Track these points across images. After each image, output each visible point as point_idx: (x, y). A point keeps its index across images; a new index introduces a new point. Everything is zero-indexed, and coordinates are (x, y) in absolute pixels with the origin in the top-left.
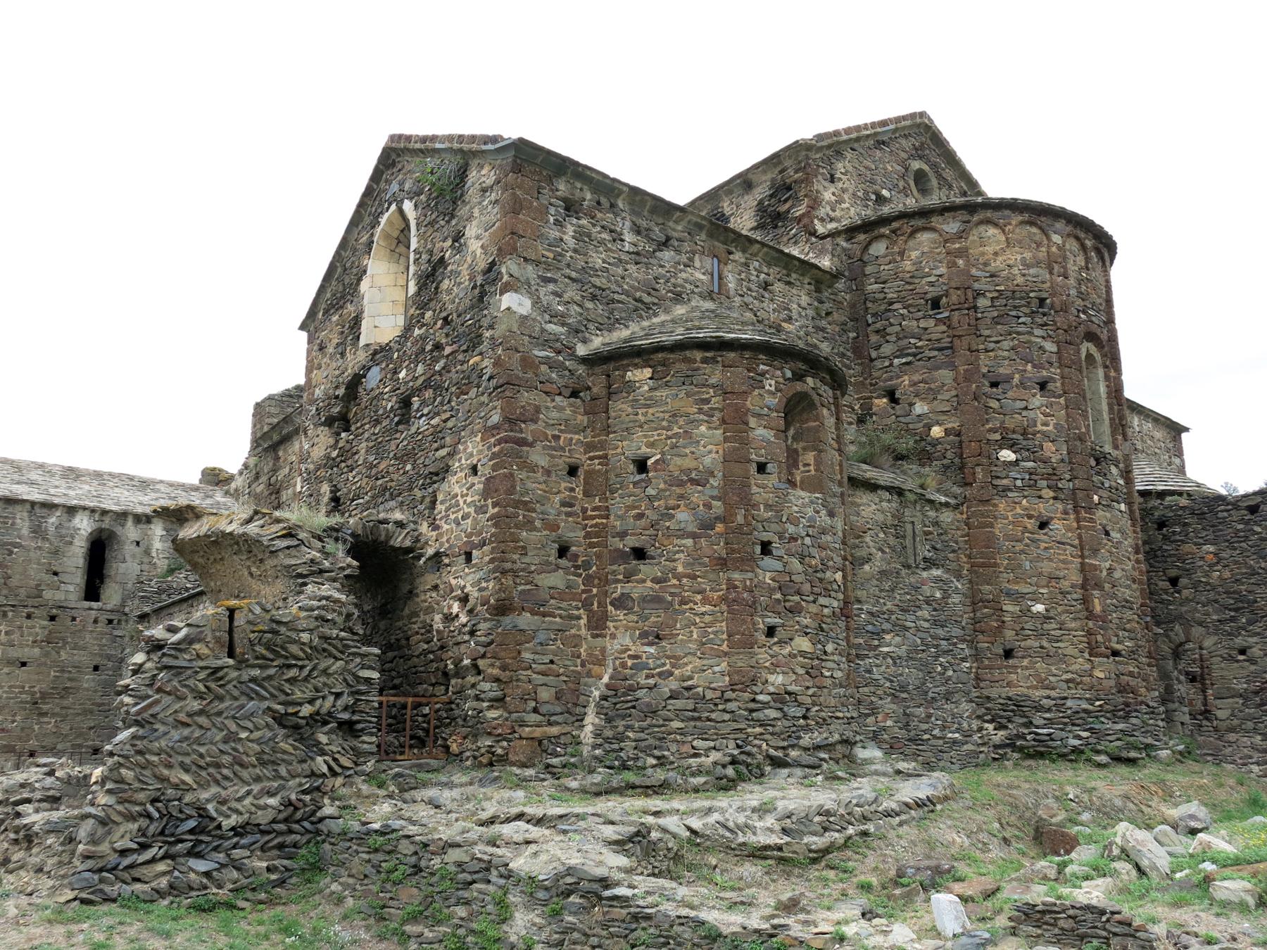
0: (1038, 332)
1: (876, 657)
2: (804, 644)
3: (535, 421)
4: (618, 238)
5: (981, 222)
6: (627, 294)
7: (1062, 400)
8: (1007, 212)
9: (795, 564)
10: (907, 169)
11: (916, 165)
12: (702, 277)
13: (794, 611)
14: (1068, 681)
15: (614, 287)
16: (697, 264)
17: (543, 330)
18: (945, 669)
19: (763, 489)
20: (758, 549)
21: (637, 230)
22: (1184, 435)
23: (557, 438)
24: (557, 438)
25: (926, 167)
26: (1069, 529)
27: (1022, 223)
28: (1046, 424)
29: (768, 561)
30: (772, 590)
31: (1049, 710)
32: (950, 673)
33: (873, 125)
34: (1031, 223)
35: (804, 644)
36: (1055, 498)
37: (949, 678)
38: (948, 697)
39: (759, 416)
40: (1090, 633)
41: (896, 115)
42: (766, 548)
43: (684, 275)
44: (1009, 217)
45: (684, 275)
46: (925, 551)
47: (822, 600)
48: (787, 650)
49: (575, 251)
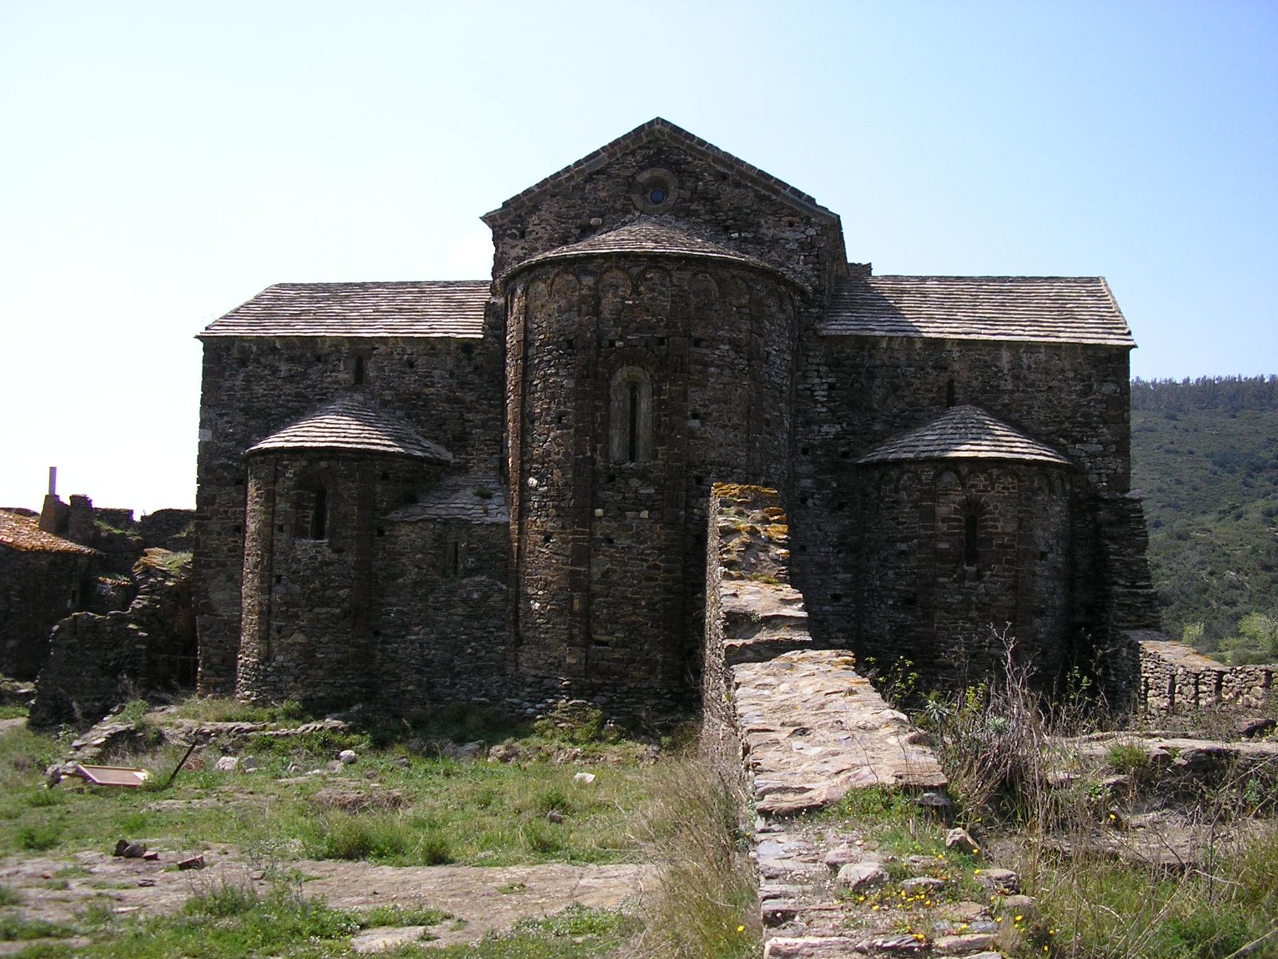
0: (562, 372)
1: (405, 642)
2: (300, 638)
3: (213, 504)
4: (275, 371)
5: (532, 281)
6: (282, 406)
7: (572, 431)
8: (548, 268)
9: (297, 588)
10: (630, 186)
12: (346, 376)
13: (296, 616)
14: (551, 664)
16: (342, 368)
17: (218, 448)
18: (477, 651)
19: (282, 540)
20: (274, 580)
21: (291, 359)
22: (1132, 352)
23: (226, 512)
24: (226, 512)
25: (661, 172)
26: (564, 541)
27: (556, 275)
28: (558, 453)
29: (278, 588)
30: (280, 605)
31: (530, 686)
32: (483, 653)
33: (578, 163)
34: (567, 272)
35: (300, 638)
36: (558, 516)
37: (481, 658)
38: (479, 670)
39: (281, 495)
40: (571, 627)
41: (611, 140)
42: (279, 578)
43: (329, 380)
44: (547, 273)
45: (329, 380)
46: (471, 562)
47: (316, 610)
48: (289, 641)
49: (244, 390)
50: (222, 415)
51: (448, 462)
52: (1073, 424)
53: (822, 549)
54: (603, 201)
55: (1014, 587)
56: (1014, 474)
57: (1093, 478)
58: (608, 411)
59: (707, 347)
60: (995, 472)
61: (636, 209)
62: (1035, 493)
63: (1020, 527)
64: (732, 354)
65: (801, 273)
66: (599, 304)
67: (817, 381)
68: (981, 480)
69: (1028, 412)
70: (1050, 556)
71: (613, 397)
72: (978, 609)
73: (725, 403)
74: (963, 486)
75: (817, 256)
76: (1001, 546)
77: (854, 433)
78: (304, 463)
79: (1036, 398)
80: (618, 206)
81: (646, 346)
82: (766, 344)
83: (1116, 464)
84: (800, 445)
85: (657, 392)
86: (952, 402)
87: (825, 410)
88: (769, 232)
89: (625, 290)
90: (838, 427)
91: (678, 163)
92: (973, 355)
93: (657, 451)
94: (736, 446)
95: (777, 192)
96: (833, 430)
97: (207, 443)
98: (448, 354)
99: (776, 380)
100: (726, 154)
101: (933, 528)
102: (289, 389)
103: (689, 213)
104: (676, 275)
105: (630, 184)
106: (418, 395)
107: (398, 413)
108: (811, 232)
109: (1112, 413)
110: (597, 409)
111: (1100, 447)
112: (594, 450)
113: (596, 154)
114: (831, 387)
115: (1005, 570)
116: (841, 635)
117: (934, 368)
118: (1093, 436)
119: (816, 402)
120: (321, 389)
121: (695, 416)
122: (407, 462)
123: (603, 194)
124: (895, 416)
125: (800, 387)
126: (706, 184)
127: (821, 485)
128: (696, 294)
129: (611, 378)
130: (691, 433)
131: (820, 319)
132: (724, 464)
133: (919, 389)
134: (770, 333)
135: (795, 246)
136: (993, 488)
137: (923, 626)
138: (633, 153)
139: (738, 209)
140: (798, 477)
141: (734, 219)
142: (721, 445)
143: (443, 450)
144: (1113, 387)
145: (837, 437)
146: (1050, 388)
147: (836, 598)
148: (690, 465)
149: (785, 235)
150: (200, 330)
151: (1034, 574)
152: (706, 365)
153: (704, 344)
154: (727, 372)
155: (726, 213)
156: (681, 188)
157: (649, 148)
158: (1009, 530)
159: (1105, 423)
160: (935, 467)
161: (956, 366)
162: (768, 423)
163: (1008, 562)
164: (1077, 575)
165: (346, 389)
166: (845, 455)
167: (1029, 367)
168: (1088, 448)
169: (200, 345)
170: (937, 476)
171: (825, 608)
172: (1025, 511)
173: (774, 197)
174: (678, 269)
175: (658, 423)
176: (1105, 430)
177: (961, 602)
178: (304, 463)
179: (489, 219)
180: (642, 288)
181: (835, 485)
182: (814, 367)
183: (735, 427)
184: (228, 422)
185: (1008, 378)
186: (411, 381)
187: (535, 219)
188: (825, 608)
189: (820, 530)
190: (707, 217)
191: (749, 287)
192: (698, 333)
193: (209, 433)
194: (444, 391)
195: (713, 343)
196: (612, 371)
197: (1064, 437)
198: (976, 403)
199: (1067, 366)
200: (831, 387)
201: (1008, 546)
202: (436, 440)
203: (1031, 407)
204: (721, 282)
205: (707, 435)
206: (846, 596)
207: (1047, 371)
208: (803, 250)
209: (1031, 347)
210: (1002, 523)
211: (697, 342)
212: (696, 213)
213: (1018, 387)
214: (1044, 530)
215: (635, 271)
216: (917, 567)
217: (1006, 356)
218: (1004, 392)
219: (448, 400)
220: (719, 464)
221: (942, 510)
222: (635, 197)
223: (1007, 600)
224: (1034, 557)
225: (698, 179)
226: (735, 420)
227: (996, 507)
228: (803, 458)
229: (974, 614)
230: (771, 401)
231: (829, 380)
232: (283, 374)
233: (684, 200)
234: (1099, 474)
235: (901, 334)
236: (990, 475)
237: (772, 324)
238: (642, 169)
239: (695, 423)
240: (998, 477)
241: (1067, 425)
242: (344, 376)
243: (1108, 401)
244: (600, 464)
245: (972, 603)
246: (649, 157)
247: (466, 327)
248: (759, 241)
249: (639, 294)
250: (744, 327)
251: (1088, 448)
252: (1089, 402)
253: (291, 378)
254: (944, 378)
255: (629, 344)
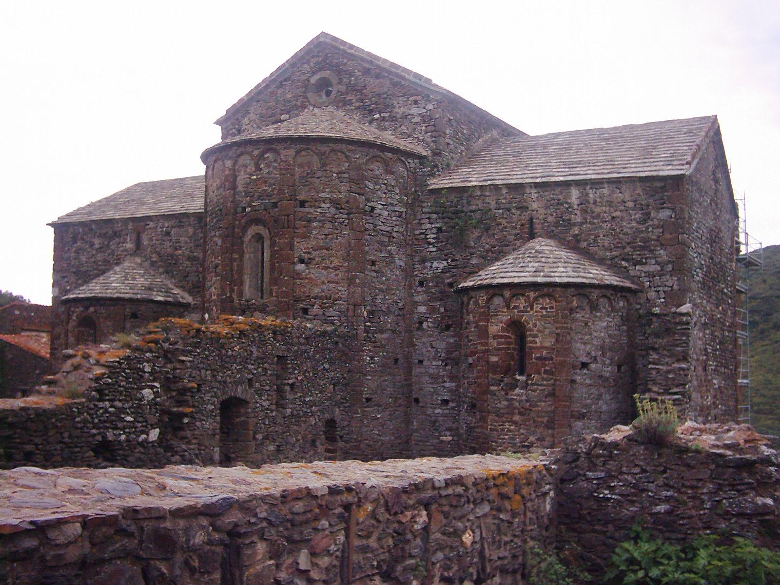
4: (92, 245)
10: (306, 87)
11: (313, 80)
15: (90, 269)
16: (129, 240)
33: (272, 75)
39: (71, 332)
43: (121, 249)
45: (121, 249)
49: (75, 259)
50: (64, 277)
51: (189, 304)
52: (634, 248)
53: (434, 363)
54: (289, 101)
55: (552, 394)
56: (549, 296)
57: (652, 294)
58: (241, 260)
59: (311, 207)
60: (532, 295)
61: (311, 104)
62: (572, 310)
63: (557, 341)
64: (333, 210)
65: (423, 140)
66: (235, 180)
67: (429, 226)
68: (522, 302)
69: (595, 241)
70: (593, 366)
71: (245, 250)
72: (520, 414)
73: (327, 249)
74: (508, 307)
75: (434, 126)
76: (537, 358)
77: (456, 267)
78: (81, 309)
79: (601, 227)
80: (299, 104)
81: (265, 210)
82: (368, 200)
83: (672, 281)
84: (417, 279)
85: (272, 245)
86: (532, 236)
87: (435, 249)
88: (400, 111)
89: (251, 168)
90: (445, 263)
91: (337, 65)
92: (548, 195)
93: (271, 290)
94: (337, 283)
95: (403, 78)
96: (441, 266)
97: (56, 297)
98: (190, 225)
99: (383, 228)
100: (369, 54)
101: (487, 344)
102: (99, 257)
103: (346, 103)
104: (283, 152)
105: (306, 85)
106: (172, 256)
107: (161, 270)
108: (430, 106)
109: (668, 236)
110: (235, 260)
111: (658, 268)
112: (232, 290)
113: (283, 65)
114: (440, 230)
115: (543, 379)
116: (448, 433)
117: (517, 208)
118: (650, 258)
119: (429, 243)
120: (117, 256)
121: (302, 261)
122: (151, 305)
123: (289, 96)
124: (488, 251)
125: (417, 232)
126: (356, 79)
127: (432, 310)
128: (301, 166)
129: (244, 235)
130: (298, 275)
131: (432, 175)
132: (326, 298)
133: (506, 227)
134: (374, 191)
135: (417, 119)
136: (532, 309)
137: (481, 427)
138: (308, 62)
139: (379, 95)
140: (416, 304)
141: (376, 103)
142: (323, 283)
143: (186, 295)
144: (668, 213)
145: (444, 271)
146: (613, 218)
147: (445, 402)
148: (297, 300)
149: (411, 112)
150: (55, 219)
151: (573, 381)
152: (310, 221)
153: (307, 204)
154: (328, 225)
155: (370, 100)
156: (339, 84)
157: (318, 57)
158: (547, 344)
159: (662, 245)
160: (487, 293)
161: (535, 206)
162: (373, 263)
163: (546, 372)
164: (639, 382)
165: (131, 255)
166: (451, 285)
167: (595, 202)
168: (646, 268)
169: (52, 229)
170: (489, 300)
171: (437, 411)
172: (562, 328)
173: (403, 83)
174: (285, 148)
175: (273, 268)
176: (662, 252)
177: (508, 406)
178: (81, 309)
179: (217, 123)
180: (262, 166)
181: (442, 310)
182: (427, 216)
183: (336, 268)
184: (67, 282)
185: (578, 212)
186: (168, 248)
187: (246, 121)
188: (437, 411)
189: (432, 347)
190: (358, 104)
191: (347, 157)
192: (301, 197)
193: (57, 290)
194: (187, 253)
195: (316, 202)
196: (244, 229)
197: (627, 260)
198: (550, 235)
199: (627, 197)
200: (440, 230)
201: (545, 359)
202: (182, 287)
203: (597, 236)
204: (321, 155)
205: (311, 275)
206: (453, 401)
207: (610, 203)
208: (424, 122)
209: (596, 184)
210: (541, 339)
211: (302, 204)
212: (350, 103)
213: (585, 219)
214: (585, 344)
215: (256, 153)
216: (477, 378)
217: (575, 193)
218: (574, 224)
219: (189, 259)
220: (321, 298)
221: (493, 329)
222: (309, 95)
223: (545, 406)
224: (574, 367)
225: (351, 76)
226: (336, 262)
227: (535, 325)
228: (419, 289)
229: (517, 418)
230: (377, 246)
231: (438, 225)
232: (97, 246)
233: (342, 94)
234: (658, 291)
235: (489, 183)
236: (528, 297)
237: (376, 184)
238: (314, 73)
239: (301, 267)
240: (536, 299)
241: (628, 249)
242: (129, 245)
243: (663, 226)
244: (236, 301)
245: (515, 408)
246: (319, 63)
247: (197, 205)
248: (393, 119)
249: (260, 170)
250: (343, 189)
251: (646, 268)
252: (647, 228)
253: (100, 249)
254: (525, 216)
255: (254, 209)
